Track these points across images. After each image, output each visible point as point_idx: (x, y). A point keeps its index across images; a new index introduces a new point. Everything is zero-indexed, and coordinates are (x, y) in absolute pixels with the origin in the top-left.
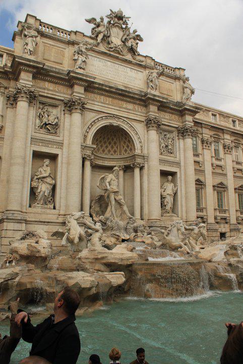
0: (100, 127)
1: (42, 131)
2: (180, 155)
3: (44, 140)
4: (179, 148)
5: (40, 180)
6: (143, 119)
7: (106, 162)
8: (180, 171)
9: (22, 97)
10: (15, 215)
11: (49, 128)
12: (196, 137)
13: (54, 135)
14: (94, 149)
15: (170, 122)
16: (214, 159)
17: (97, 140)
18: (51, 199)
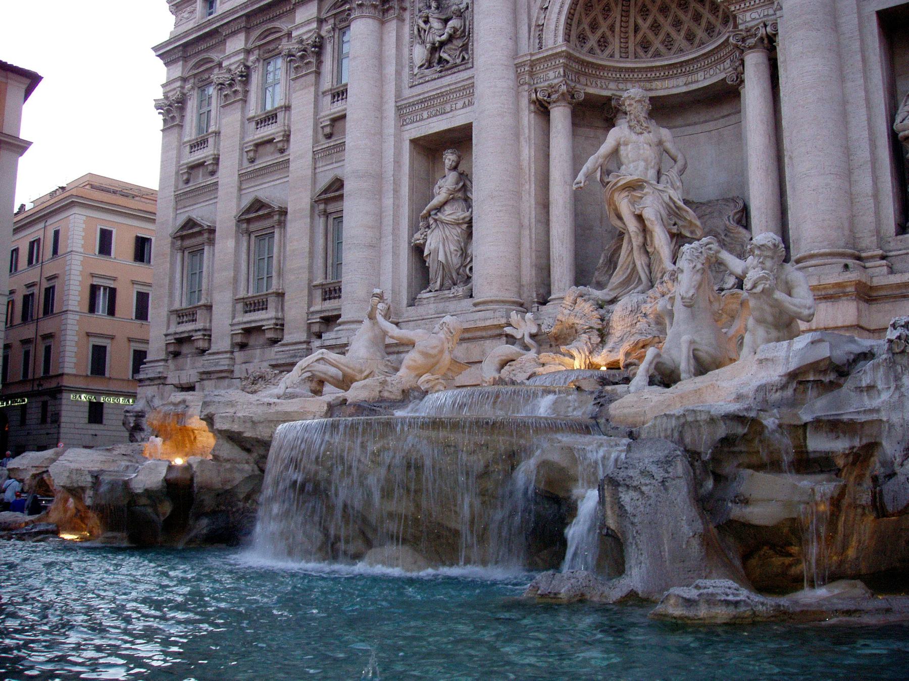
5: (431, 222)
7: (700, 75)
10: (340, 334)
11: (445, 56)
14: (569, 56)
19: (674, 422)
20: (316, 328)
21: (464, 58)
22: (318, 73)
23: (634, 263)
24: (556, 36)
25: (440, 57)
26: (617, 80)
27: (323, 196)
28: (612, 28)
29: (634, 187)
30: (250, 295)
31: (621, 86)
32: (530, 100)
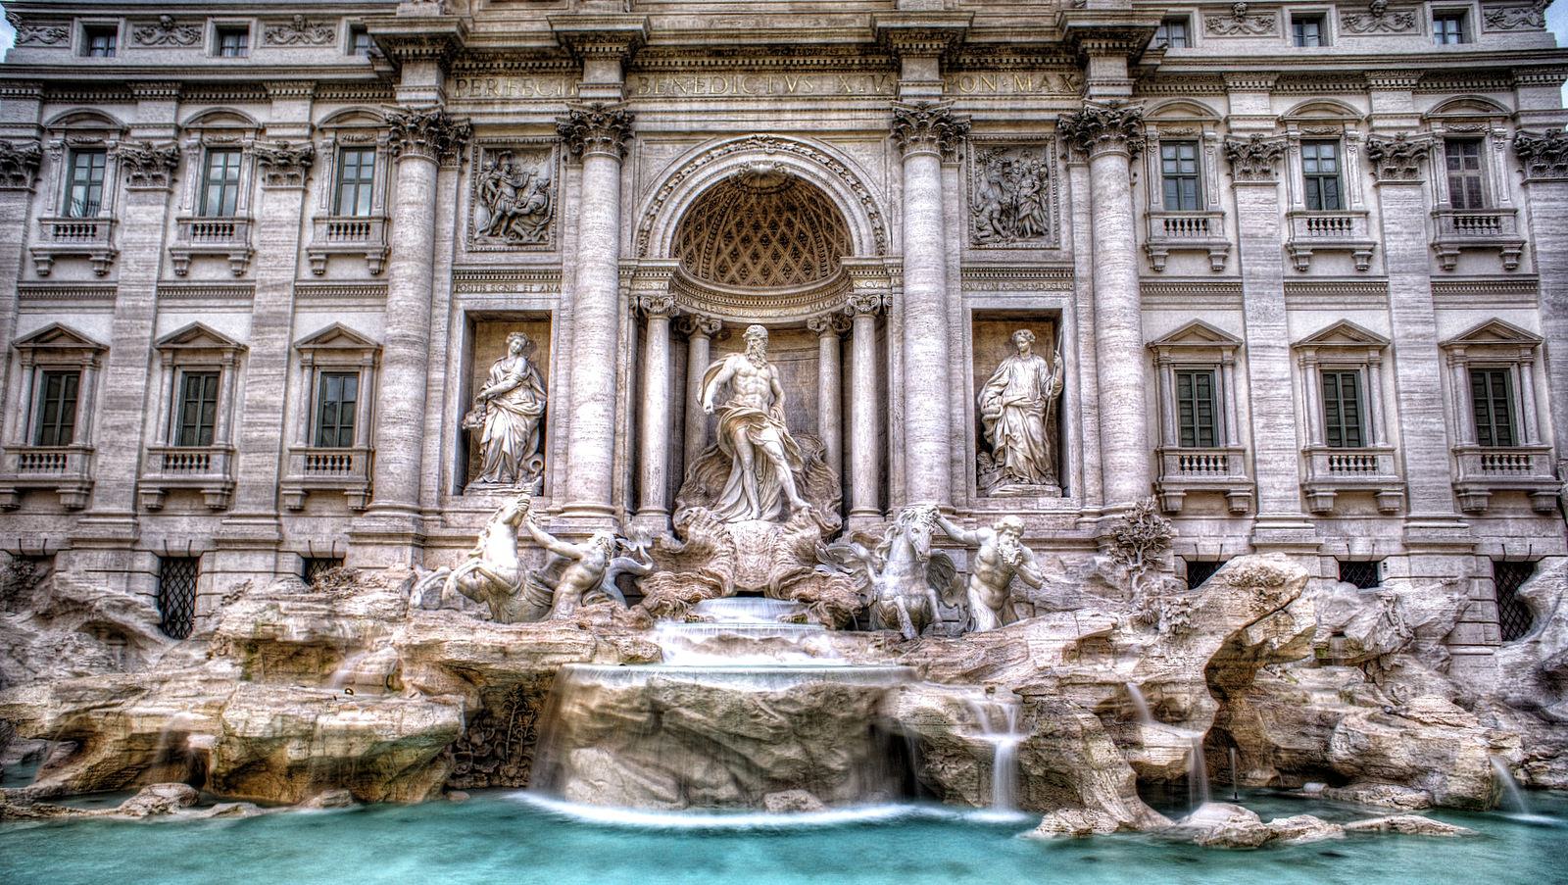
0: (702, 188)
1: (497, 243)
3: (499, 272)
4: (1070, 205)
6: (882, 121)
9: (406, 144)
11: (519, 229)
12: (1193, 143)
13: (533, 248)
14: (677, 274)
15: (1020, 105)
16: (1301, 225)
17: (729, 237)
20: (296, 502)
21: (542, 237)
22: (305, 192)
24: (662, 247)
25: (508, 227)
26: (700, 299)
27: (311, 346)
28: (699, 246)
29: (753, 420)
30: (171, 445)
31: (703, 306)
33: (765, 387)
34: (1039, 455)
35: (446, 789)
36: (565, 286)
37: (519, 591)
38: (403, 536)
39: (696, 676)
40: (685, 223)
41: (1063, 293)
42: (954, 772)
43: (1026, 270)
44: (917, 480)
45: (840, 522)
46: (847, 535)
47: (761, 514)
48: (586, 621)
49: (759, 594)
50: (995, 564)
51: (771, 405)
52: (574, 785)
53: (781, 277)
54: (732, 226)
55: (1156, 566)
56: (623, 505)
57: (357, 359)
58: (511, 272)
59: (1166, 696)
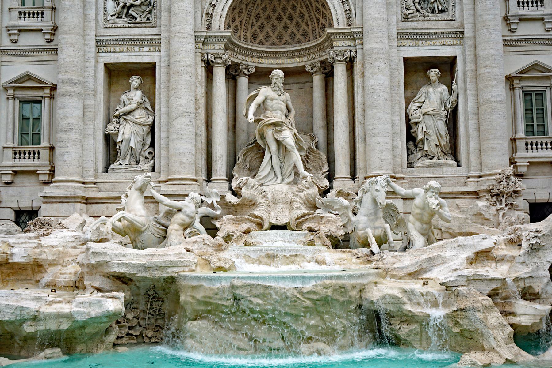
2: (462, 11)
3: (124, 40)
5: (122, 120)
8: (463, 53)
11: (134, 14)
13: (143, 25)
17: (258, 17)
18: (150, 153)
19: (466, 279)
20: (8, 178)
23: (272, 166)
25: (128, 12)
26: (242, 54)
29: (277, 125)
31: (244, 58)
32: (202, 59)
33: (284, 107)
34: (443, 143)
35: (114, 345)
36: (163, 47)
37: (148, 229)
38: (75, 197)
39: (258, 278)
40: (233, 8)
41: (457, 47)
42: (407, 330)
43: (435, 33)
44: (373, 159)
45: (327, 183)
46: (333, 192)
47: (283, 180)
48: (189, 247)
49: (283, 227)
50: (423, 209)
51: (286, 116)
52: (189, 342)
53: (289, 39)
54: (260, 10)
55: (512, 206)
56: (203, 176)
57: (40, 93)
58: (131, 40)
59: (527, 285)
